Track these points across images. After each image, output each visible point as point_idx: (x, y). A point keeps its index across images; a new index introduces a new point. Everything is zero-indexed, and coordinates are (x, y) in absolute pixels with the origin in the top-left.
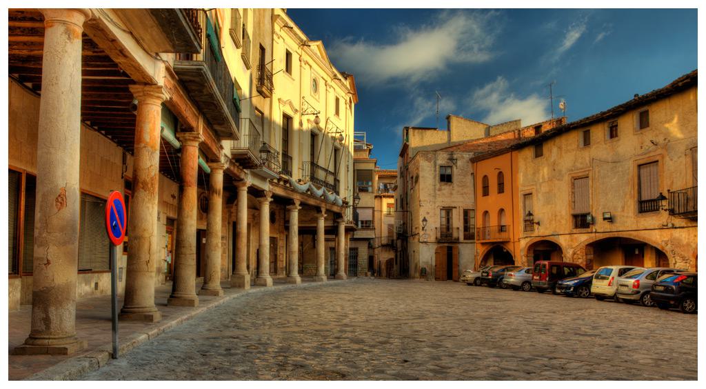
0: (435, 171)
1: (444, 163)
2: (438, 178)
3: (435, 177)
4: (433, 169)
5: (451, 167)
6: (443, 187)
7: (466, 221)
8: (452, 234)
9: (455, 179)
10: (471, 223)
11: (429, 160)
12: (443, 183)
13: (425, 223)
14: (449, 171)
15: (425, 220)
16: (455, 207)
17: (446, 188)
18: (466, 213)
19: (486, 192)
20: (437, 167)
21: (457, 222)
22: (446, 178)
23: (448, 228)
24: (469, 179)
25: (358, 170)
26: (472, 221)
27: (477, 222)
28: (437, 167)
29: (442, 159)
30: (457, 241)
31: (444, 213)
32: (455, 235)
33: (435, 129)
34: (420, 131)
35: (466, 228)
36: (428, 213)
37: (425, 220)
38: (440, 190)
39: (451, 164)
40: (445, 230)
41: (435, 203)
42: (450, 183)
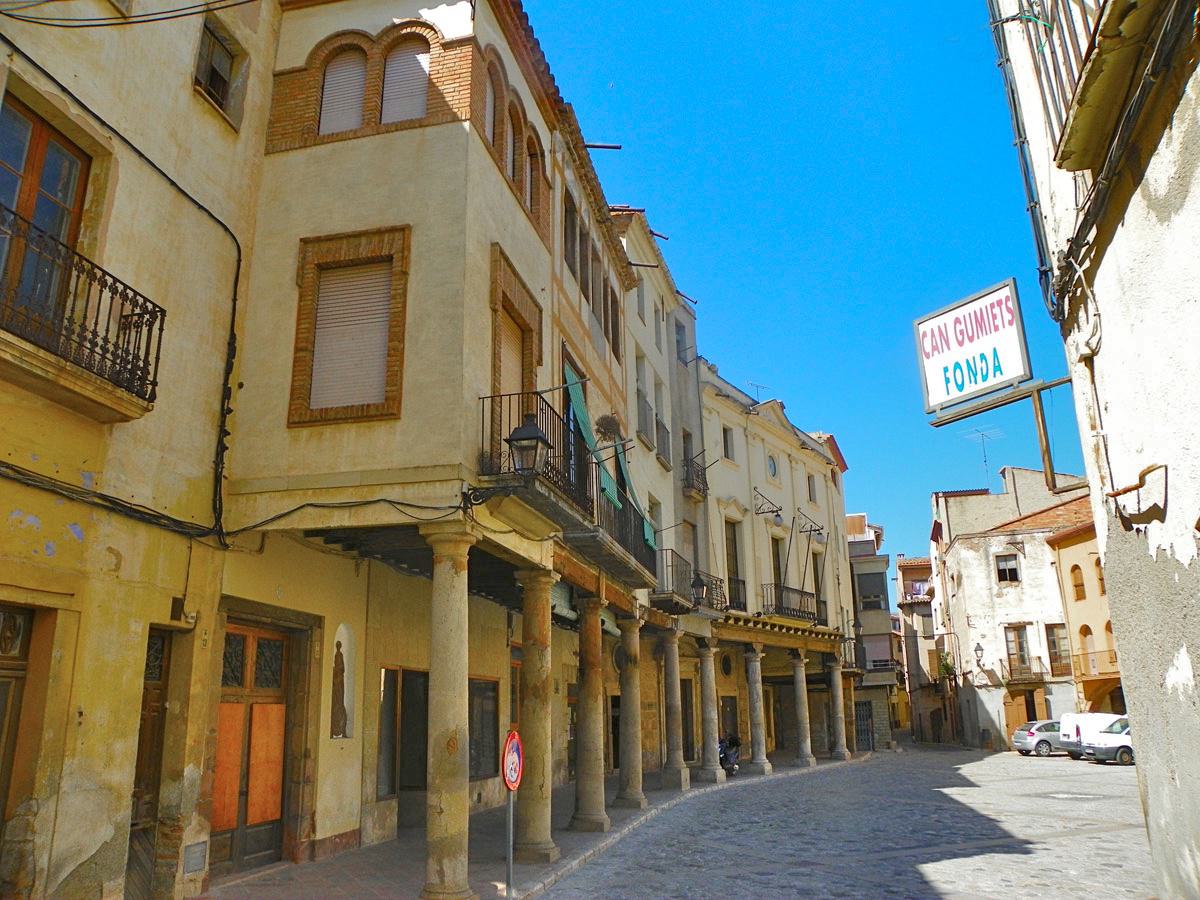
0: (988, 565)
1: (1001, 549)
2: (994, 576)
3: (989, 576)
4: (983, 561)
5: (1016, 555)
6: (1005, 591)
7: (1052, 644)
8: (1029, 668)
9: (1023, 574)
12: (1004, 583)
13: (979, 652)
14: (1011, 564)
15: (979, 648)
16: (1031, 623)
17: (1010, 591)
18: (1050, 629)
19: (1080, 593)
20: (991, 558)
21: (1037, 646)
22: (1009, 576)
23: (1022, 660)
24: (1050, 574)
25: (859, 575)
26: (1064, 645)
27: (1071, 643)
28: (991, 558)
29: (998, 545)
30: (1040, 682)
31: (1012, 636)
32: (1036, 668)
33: (985, 492)
35: (1054, 657)
36: (984, 636)
37: (979, 648)
38: (999, 595)
39: (1013, 550)
40: (1016, 664)
41: (993, 617)
42: (1016, 583)
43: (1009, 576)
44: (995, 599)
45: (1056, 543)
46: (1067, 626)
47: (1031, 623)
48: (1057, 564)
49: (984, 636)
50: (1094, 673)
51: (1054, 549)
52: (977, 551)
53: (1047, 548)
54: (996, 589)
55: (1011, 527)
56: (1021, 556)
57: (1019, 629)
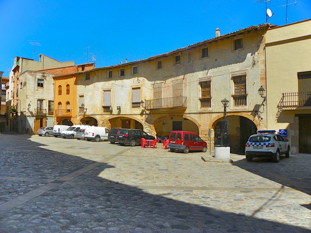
0: (35, 81)
2: (36, 84)
3: (35, 84)
4: (34, 80)
8: (42, 112)
9: (45, 85)
10: (52, 107)
11: (32, 75)
12: (39, 87)
14: (42, 82)
15: (29, 105)
16: (45, 100)
17: (40, 89)
18: (50, 102)
21: (45, 106)
22: (40, 85)
23: (41, 109)
24: (52, 87)
26: (52, 107)
27: (55, 106)
29: (39, 76)
30: (45, 116)
31: (39, 102)
32: (44, 112)
33: (33, 60)
34: (26, 60)
35: (49, 110)
36: (31, 102)
37: (29, 105)
38: (37, 90)
39: (43, 78)
40: (39, 110)
41: (34, 97)
42: (42, 88)
43: (40, 85)
44: (36, 91)
45: (55, 78)
46: (54, 101)
47: (45, 100)
48: (54, 84)
49: (31, 102)
50: (60, 115)
51: (54, 80)
52: (33, 76)
53: (53, 79)
54: (36, 88)
55: (44, 71)
56: (45, 80)
57: (41, 101)
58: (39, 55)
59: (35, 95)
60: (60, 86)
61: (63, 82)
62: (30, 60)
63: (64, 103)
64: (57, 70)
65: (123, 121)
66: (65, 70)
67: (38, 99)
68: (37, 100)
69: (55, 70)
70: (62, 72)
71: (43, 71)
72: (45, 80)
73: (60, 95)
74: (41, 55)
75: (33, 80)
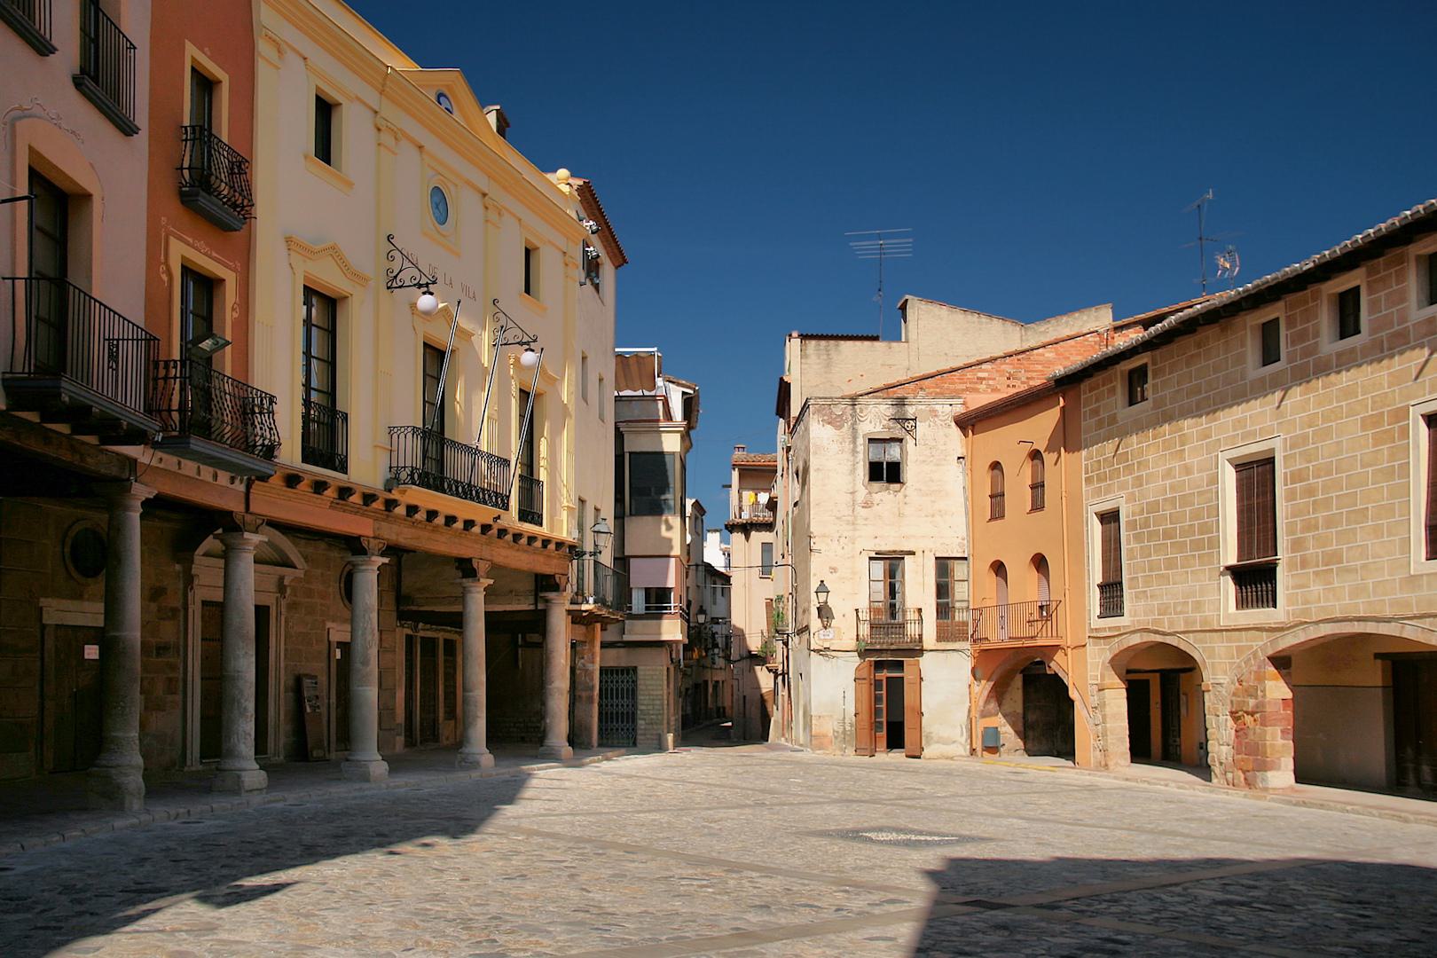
0: (854, 452)
1: (879, 429)
2: (862, 472)
3: (853, 471)
4: (848, 446)
5: (901, 440)
6: (877, 497)
7: (943, 590)
9: (909, 473)
10: (958, 596)
11: (835, 422)
12: (876, 485)
13: (822, 597)
14: (894, 453)
16: (913, 553)
17: (884, 495)
19: (997, 513)
20: (860, 441)
21: (919, 591)
22: (886, 473)
25: (630, 453)
28: (860, 441)
29: (875, 418)
31: (879, 568)
33: (875, 338)
34: (823, 343)
35: (943, 611)
36: (834, 570)
38: (867, 505)
39: (898, 433)
42: (897, 486)
43: (886, 473)
44: (859, 509)
45: (969, 423)
46: (971, 559)
47: (913, 553)
48: (968, 459)
49: (834, 570)
50: (998, 636)
51: (966, 435)
52: (839, 428)
53: (955, 431)
54: (862, 492)
55: (900, 392)
56: (909, 441)
57: (893, 562)
58: (899, 305)
59: (855, 530)
60: (996, 466)
61: (1010, 441)
62: (842, 342)
63: (1020, 569)
64: (981, 375)
65: (1394, 663)
66: (1032, 367)
67: (873, 555)
68: (871, 559)
69: (969, 374)
70: (1011, 382)
71: (896, 394)
72: (908, 437)
73: (999, 522)
74: (907, 300)
75: (843, 451)
